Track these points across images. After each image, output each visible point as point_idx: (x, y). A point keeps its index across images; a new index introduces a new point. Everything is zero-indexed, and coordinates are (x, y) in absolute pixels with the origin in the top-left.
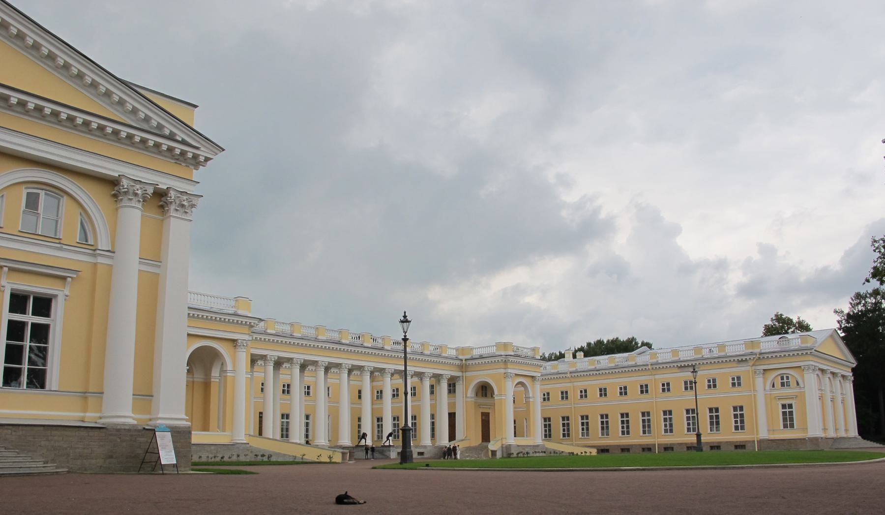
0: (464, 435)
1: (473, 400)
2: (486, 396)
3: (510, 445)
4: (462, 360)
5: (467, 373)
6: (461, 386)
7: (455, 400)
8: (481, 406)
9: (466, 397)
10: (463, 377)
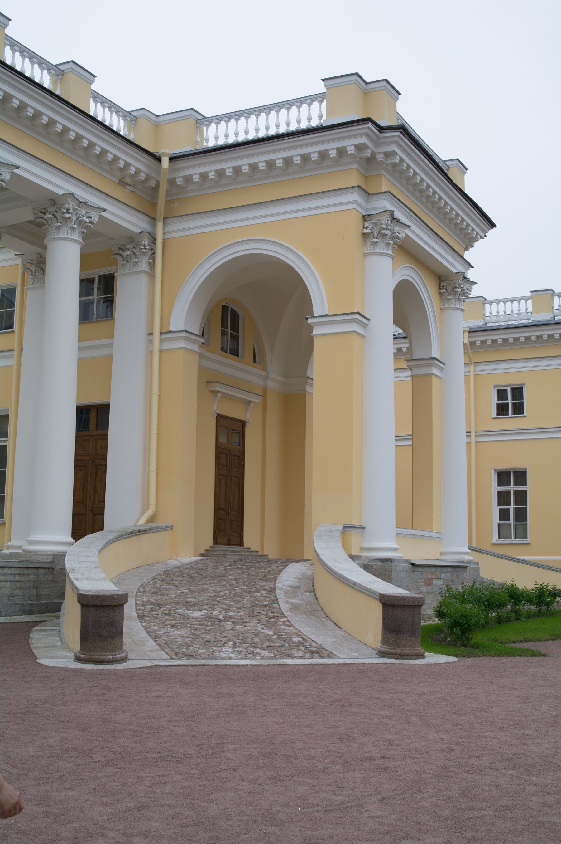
0: (145, 508)
1: (196, 348)
2: (235, 352)
3: (384, 560)
4: (158, 159)
5: (172, 227)
6: (144, 279)
7: (111, 345)
8: (218, 388)
9: (161, 333)
10: (154, 240)
